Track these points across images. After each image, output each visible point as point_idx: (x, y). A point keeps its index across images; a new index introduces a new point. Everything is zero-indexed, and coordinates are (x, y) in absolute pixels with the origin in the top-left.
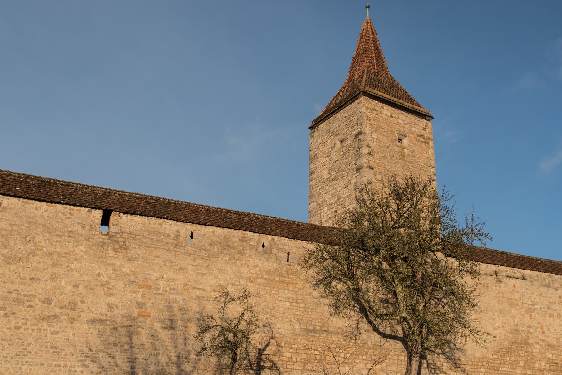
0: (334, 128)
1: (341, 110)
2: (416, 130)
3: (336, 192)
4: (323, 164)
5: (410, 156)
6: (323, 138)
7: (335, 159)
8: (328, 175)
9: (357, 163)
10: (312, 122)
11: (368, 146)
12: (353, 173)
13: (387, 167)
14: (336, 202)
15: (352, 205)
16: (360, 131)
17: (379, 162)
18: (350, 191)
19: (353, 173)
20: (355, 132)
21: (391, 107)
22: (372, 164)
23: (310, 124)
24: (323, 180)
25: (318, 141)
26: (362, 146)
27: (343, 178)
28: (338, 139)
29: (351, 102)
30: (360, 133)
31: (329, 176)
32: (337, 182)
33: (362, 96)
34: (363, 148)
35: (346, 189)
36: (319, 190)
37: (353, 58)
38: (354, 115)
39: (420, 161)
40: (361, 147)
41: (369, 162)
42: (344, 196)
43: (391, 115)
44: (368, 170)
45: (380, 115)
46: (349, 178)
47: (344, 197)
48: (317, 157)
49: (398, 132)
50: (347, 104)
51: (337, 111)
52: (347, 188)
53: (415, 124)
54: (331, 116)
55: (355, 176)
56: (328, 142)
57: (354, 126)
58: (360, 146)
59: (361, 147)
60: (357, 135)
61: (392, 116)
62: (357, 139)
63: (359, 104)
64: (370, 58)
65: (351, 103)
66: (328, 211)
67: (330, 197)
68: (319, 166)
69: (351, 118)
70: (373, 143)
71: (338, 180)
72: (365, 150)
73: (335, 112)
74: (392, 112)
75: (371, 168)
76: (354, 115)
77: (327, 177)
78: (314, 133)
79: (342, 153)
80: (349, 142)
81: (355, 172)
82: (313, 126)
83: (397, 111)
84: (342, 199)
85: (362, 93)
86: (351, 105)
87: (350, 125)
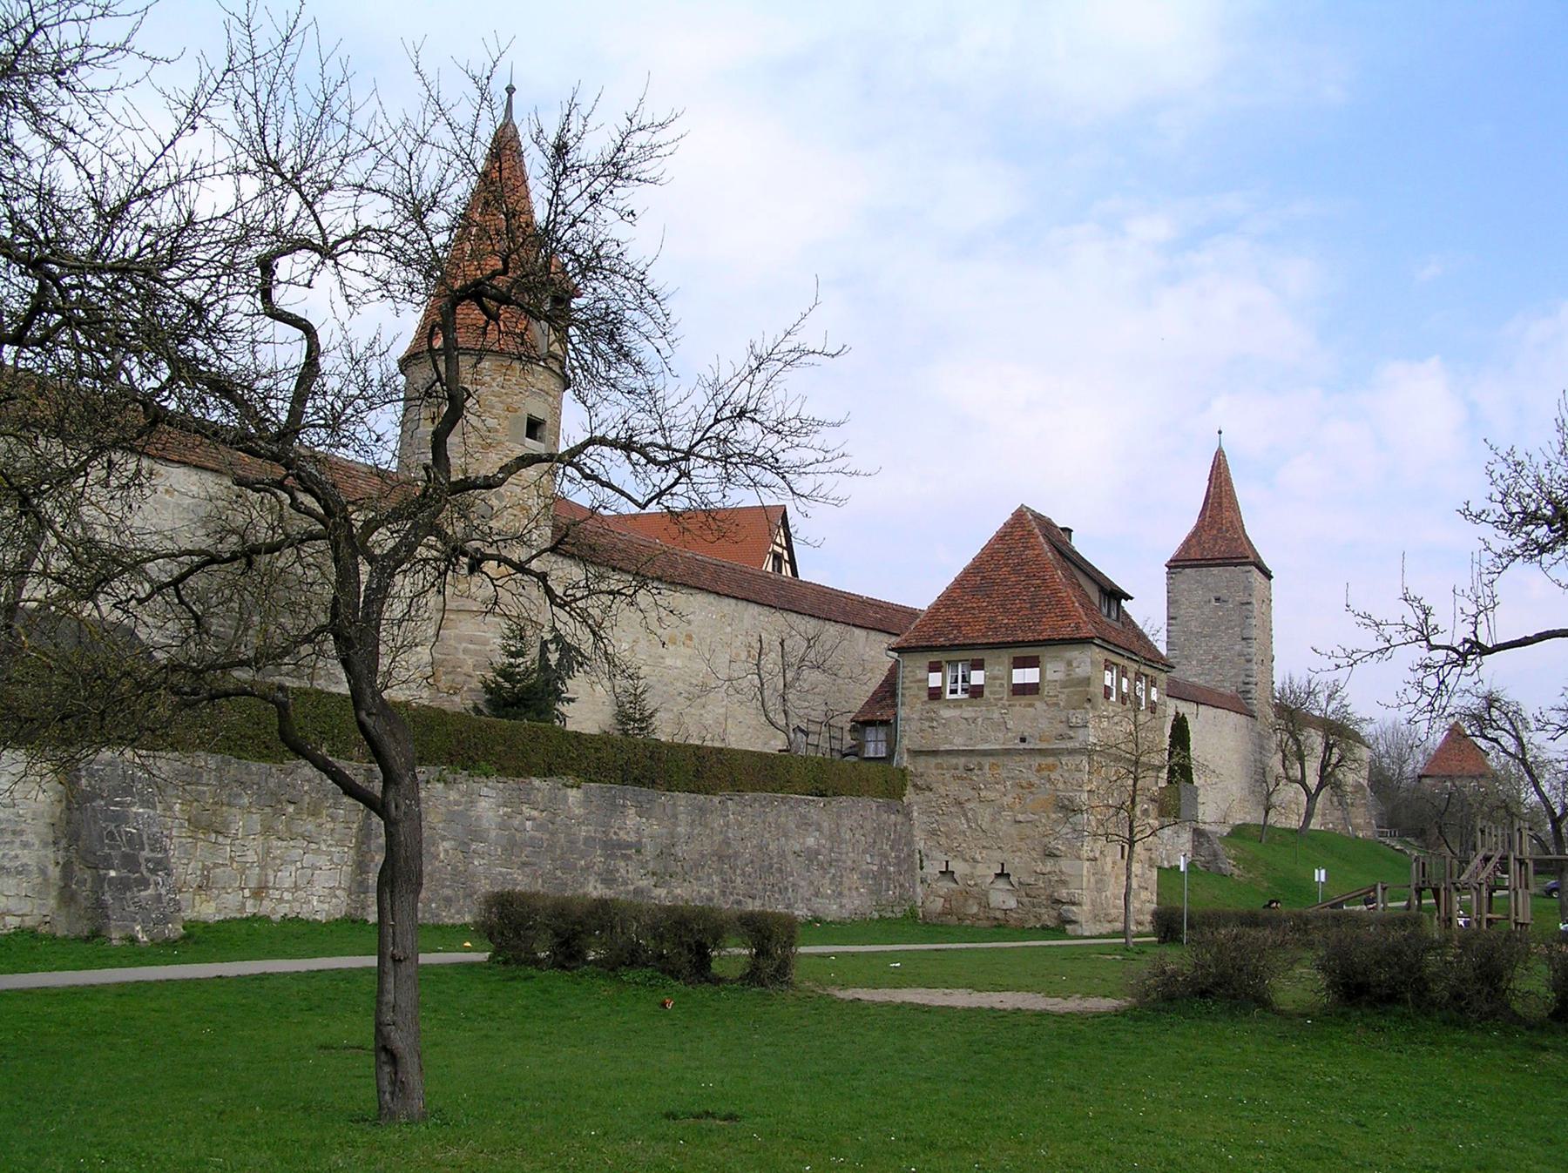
30: (1248, 603)
46: (1231, 643)
67: (1201, 652)
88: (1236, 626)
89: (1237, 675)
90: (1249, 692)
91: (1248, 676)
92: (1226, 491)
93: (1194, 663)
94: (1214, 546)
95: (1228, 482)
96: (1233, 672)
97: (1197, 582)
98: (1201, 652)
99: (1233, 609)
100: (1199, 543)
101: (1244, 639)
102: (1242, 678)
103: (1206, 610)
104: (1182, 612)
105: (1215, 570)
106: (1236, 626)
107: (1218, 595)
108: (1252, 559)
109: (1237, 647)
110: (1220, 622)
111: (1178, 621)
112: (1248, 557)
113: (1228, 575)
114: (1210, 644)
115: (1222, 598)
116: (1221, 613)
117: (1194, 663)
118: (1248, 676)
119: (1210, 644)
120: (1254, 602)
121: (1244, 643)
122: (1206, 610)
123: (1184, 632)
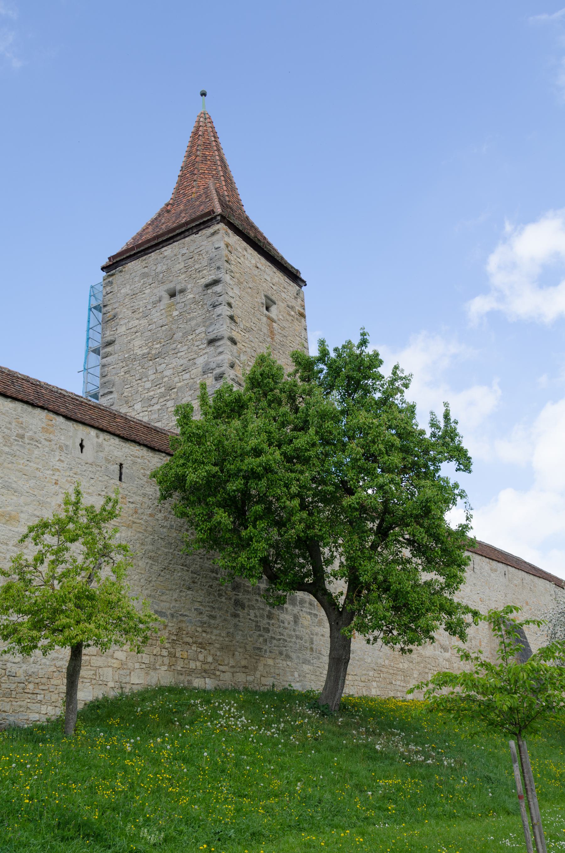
0: (157, 271)
1: (174, 242)
2: (286, 296)
3: (163, 378)
4: (132, 330)
5: (281, 335)
6: (133, 287)
7: (161, 322)
8: (144, 348)
9: (210, 330)
10: (109, 258)
11: (230, 305)
12: (200, 347)
13: (253, 345)
14: (162, 395)
16: (215, 278)
17: (243, 334)
18: (192, 377)
19: (200, 347)
20: (203, 280)
21: (256, 252)
22: (235, 335)
23: (105, 261)
24: (132, 357)
25: (122, 291)
26: (221, 304)
27: (179, 355)
28: (167, 291)
29: (195, 231)
30: (216, 282)
31: (146, 351)
32: (166, 361)
33: (218, 223)
34: (221, 307)
35: (183, 373)
36: (123, 374)
37: (182, 167)
39: (292, 346)
40: (217, 305)
41: (231, 332)
42: (179, 384)
43: (256, 264)
44: (229, 343)
45: (242, 259)
47: (181, 387)
48: (120, 317)
49: (265, 293)
50: (187, 233)
51: (164, 244)
52: (187, 371)
53: (285, 288)
54: (151, 251)
55: (204, 352)
56: (144, 293)
57: (202, 271)
58: (217, 303)
59: (217, 305)
60: (208, 286)
61: (258, 266)
62: (209, 291)
64: (214, 172)
65: (197, 233)
66: (145, 409)
68: (124, 333)
69: (196, 257)
70: (235, 302)
71: (167, 358)
72: (224, 310)
73: (161, 246)
74: (258, 260)
75: (234, 342)
76: (201, 253)
77: (141, 353)
78: (114, 277)
79: (175, 313)
80: (192, 296)
81: (205, 345)
82: (110, 265)
83: (263, 260)
84: (175, 390)
85: (219, 218)
86: (194, 235)
87: (193, 268)
88: (198, 325)
92: (204, 156)
97: (145, 275)
98: (148, 385)
99: (195, 302)
101: (211, 342)
105: (168, 251)
106: (198, 325)
107: (171, 286)
108: (219, 210)
109: (200, 361)
110: (174, 327)
113: (184, 251)
114: (160, 368)
115: (178, 288)
119: (160, 368)
120: (227, 278)
122: (156, 315)
123: (124, 360)
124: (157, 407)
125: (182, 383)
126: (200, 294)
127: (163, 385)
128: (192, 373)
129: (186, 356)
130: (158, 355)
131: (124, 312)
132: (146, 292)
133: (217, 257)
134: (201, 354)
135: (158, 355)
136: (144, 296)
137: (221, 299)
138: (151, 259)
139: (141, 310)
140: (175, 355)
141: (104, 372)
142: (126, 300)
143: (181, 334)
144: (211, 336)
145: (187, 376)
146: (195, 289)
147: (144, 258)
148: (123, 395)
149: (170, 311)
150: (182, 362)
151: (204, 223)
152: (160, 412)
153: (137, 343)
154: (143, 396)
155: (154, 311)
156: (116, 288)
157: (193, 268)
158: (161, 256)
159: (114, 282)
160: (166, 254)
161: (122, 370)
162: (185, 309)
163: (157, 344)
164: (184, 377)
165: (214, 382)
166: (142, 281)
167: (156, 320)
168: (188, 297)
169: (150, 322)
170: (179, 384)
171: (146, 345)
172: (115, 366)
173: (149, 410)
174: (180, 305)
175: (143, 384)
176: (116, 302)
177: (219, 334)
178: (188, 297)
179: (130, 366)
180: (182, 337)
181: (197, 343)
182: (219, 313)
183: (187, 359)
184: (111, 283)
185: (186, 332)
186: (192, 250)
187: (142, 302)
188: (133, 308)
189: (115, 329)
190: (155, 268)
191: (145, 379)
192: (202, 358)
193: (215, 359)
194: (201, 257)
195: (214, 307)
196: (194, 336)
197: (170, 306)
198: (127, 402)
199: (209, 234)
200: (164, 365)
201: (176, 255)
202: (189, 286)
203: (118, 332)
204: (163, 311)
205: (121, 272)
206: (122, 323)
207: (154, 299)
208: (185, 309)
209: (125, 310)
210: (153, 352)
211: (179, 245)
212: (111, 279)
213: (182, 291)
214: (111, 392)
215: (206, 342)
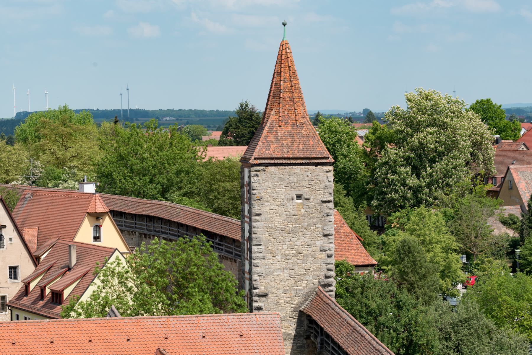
8: (282, 225)
15: (318, 264)
19: (319, 235)
24: (274, 227)
25: (266, 184)
27: (305, 236)
30: (329, 202)
34: (331, 217)
36: (268, 235)
38: (320, 179)
42: (305, 252)
47: (306, 254)
50: (311, 164)
55: (321, 239)
60: (324, 202)
62: (324, 205)
63: (327, 172)
65: (316, 166)
66: (283, 260)
67: (285, 247)
77: (280, 226)
78: (259, 172)
80: (313, 204)
87: (314, 187)
89: (319, 269)
90: (330, 285)
91: (330, 270)
93: (278, 257)
94: (292, 143)
95: (293, 75)
96: (315, 266)
97: (281, 179)
100: (277, 139)
101: (325, 236)
102: (324, 272)
103: (289, 207)
104: (267, 209)
105: (297, 169)
109: (319, 243)
111: (262, 218)
112: (327, 158)
113: (309, 174)
116: (303, 211)
117: (278, 257)
118: (330, 270)
121: (325, 239)
124: (290, 261)
125: (307, 252)
126: (319, 205)
127: (295, 249)
128: (313, 248)
129: (310, 237)
130: (292, 232)
131: (266, 197)
132: (283, 190)
133: (330, 186)
134: (319, 239)
135: (292, 232)
136: (281, 192)
137: (331, 211)
138: (285, 170)
139: (279, 201)
140: (303, 235)
141: (255, 231)
142: (269, 191)
143: (306, 224)
144: (327, 233)
145: (310, 249)
146: (315, 200)
147: (281, 167)
148: (268, 248)
149: (299, 208)
150: (307, 240)
151: (323, 163)
152: (293, 264)
153: (277, 219)
154: (282, 252)
155: (288, 204)
156: (261, 180)
157: (314, 187)
158: (293, 171)
159: (259, 175)
160: (296, 171)
161: (267, 233)
162: (309, 210)
163: (290, 224)
164: (308, 249)
165: (326, 257)
166: (280, 182)
167: (290, 210)
168: (311, 203)
169: (286, 210)
170: (305, 252)
171: (283, 223)
172: (262, 229)
173: (286, 261)
174: (306, 206)
175: (282, 245)
176: (261, 189)
177: (331, 232)
178: (311, 203)
179: (273, 233)
180: (307, 226)
181: (317, 233)
182: (331, 220)
183: (310, 240)
184: (257, 176)
185: (309, 224)
186: (314, 176)
187: (279, 196)
188: (274, 197)
189: (261, 206)
190: (288, 177)
191: (284, 243)
192: (319, 242)
193: (327, 245)
194: (318, 182)
195: (328, 216)
196: (315, 228)
197: (298, 204)
198: (271, 253)
199: (325, 171)
200: (295, 239)
201: (303, 175)
202: (312, 197)
203: (264, 208)
204: (295, 207)
205: (265, 171)
206: (266, 204)
207: (288, 196)
208: (309, 210)
209: (268, 197)
210: (288, 228)
211: (305, 168)
212: (258, 173)
213: (307, 199)
214: (260, 245)
215: (322, 234)
